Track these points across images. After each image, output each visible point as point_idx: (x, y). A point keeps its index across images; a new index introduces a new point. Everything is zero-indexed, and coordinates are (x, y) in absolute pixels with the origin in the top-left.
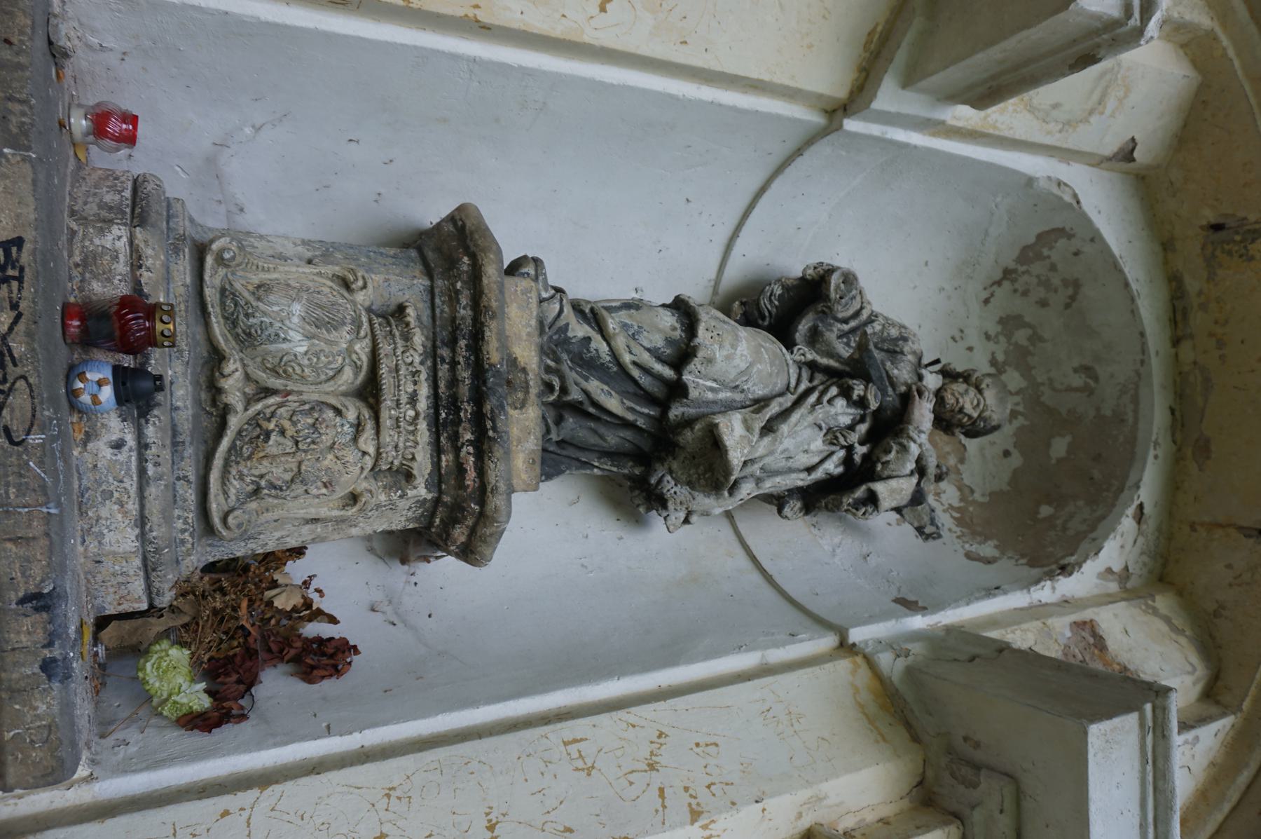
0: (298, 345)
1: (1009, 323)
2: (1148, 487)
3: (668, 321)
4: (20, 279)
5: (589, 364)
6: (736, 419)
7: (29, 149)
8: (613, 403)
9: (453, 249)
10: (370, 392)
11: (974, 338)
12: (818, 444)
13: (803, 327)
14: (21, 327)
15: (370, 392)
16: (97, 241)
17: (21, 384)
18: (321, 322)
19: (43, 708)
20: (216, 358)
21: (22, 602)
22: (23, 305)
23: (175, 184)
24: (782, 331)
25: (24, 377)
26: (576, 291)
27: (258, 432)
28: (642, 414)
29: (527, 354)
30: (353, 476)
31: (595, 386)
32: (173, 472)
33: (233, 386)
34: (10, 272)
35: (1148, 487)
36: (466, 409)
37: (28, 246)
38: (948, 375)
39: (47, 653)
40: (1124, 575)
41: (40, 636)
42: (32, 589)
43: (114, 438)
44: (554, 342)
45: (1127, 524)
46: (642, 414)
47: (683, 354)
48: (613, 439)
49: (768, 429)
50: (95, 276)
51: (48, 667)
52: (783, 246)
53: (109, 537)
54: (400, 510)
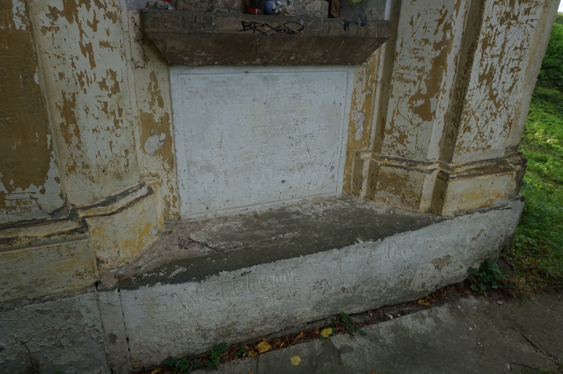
4: (255, 23)
7: (212, 17)
14: (269, 24)
16: (220, 3)
17: (286, 25)
19: (373, 27)
21: (345, 30)
22: (263, 23)
25: (284, 24)
34: (253, 26)
37: (244, 20)
39: (359, 25)
41: (355, 26)
42: (343, 27)
43: (286, 4)
50: (232, 5)
51: (363, 25)
53: (316, 9)
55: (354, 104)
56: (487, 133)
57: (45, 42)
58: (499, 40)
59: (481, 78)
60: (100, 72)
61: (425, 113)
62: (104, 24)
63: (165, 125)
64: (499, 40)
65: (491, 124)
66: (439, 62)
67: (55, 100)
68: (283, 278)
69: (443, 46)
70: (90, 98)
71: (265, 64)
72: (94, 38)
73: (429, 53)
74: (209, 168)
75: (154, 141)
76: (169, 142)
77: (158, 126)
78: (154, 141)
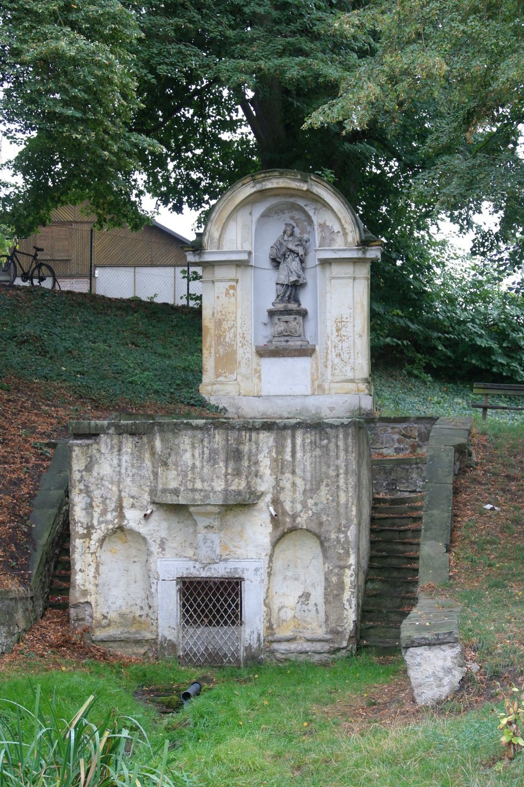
0: (282, 328)
1: (276, 213)
2: (301, 203)
3: (278, 286)
5: (284, 295)
6: (291, 278)
8: (288, 293)
9: (271, 314)
10: (287, 322)
11: (279, 217)
12: (294, 263)
13: (278, 260)
15: (287, 322)
18: (280, 326)
20: (284, 336)
23: (267, 340)
24: (279, 263)
26: (275, 298)
27: (290, 332)
28: (290, 289)
29: (283, 305)
30: (295, 323)
31: (287, 295)
32: (293, 339)
33: (286, 334)
35: (301, 203)
36: (288, 312)
38: (285, 232)
40: (315, 209)
44: (282, 301)
45: (307, 209)
46: (290, 289)
47: (283, 285)
48: (293, 291)
49: (292, 272)
52: (267, 263)
54: (300, 319)
55: (312, 367)
56: (344, 371)
57: (238, 351)
58: (340, 346)
59: (336, 355)
60: (246, 357)
61: (326, 366)
62: (248, 349)
63: (260, 371)
64: (340, 346)
65: (345, 368)
66: (327, 353)
67: (238, 361)
68: (279, 401)
69: (327, 349)
70: (244, 361)
71: (283, 356)
72: (246, 351)
73: (325, 351)
74: (269, 383)
75: (257, 375)
76: (260, 375)
77: (258, 372)
78: (257, 375)
